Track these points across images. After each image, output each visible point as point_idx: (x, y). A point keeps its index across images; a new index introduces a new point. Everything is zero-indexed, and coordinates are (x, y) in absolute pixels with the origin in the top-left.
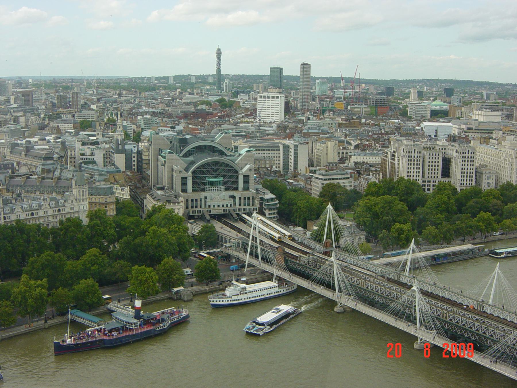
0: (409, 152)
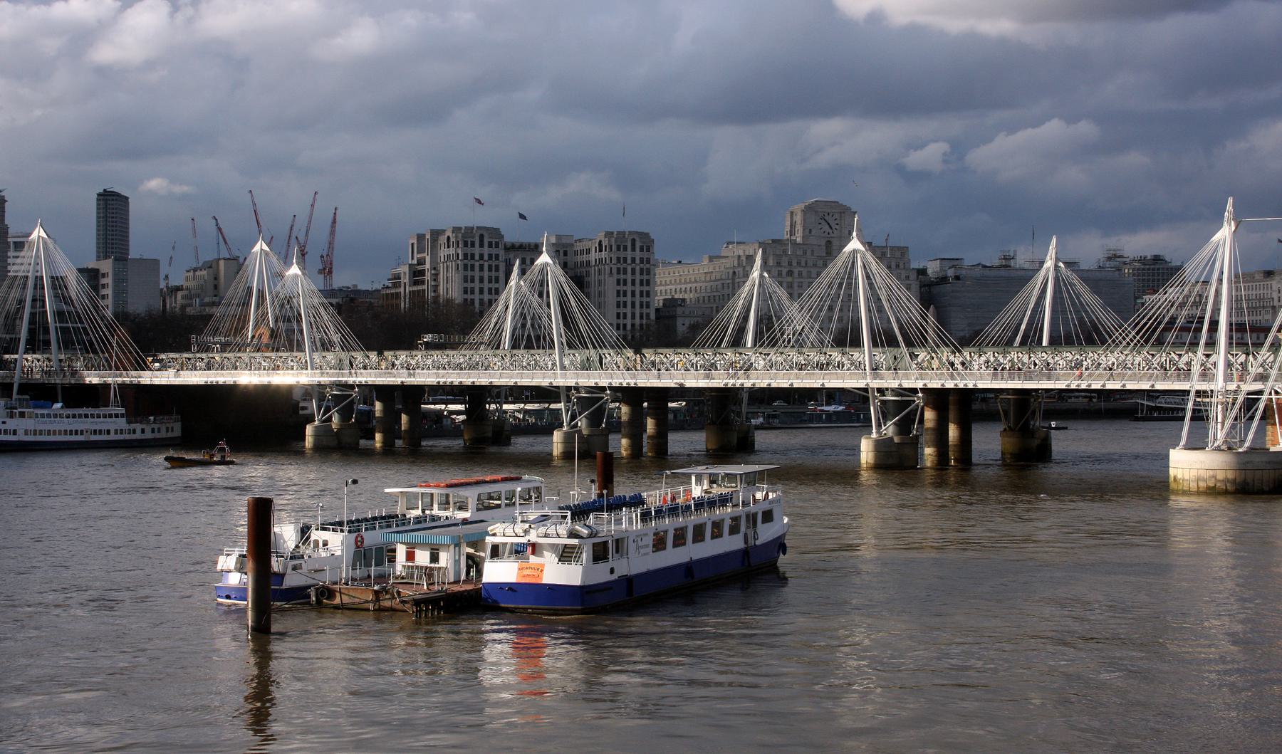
0: (466, 244)
